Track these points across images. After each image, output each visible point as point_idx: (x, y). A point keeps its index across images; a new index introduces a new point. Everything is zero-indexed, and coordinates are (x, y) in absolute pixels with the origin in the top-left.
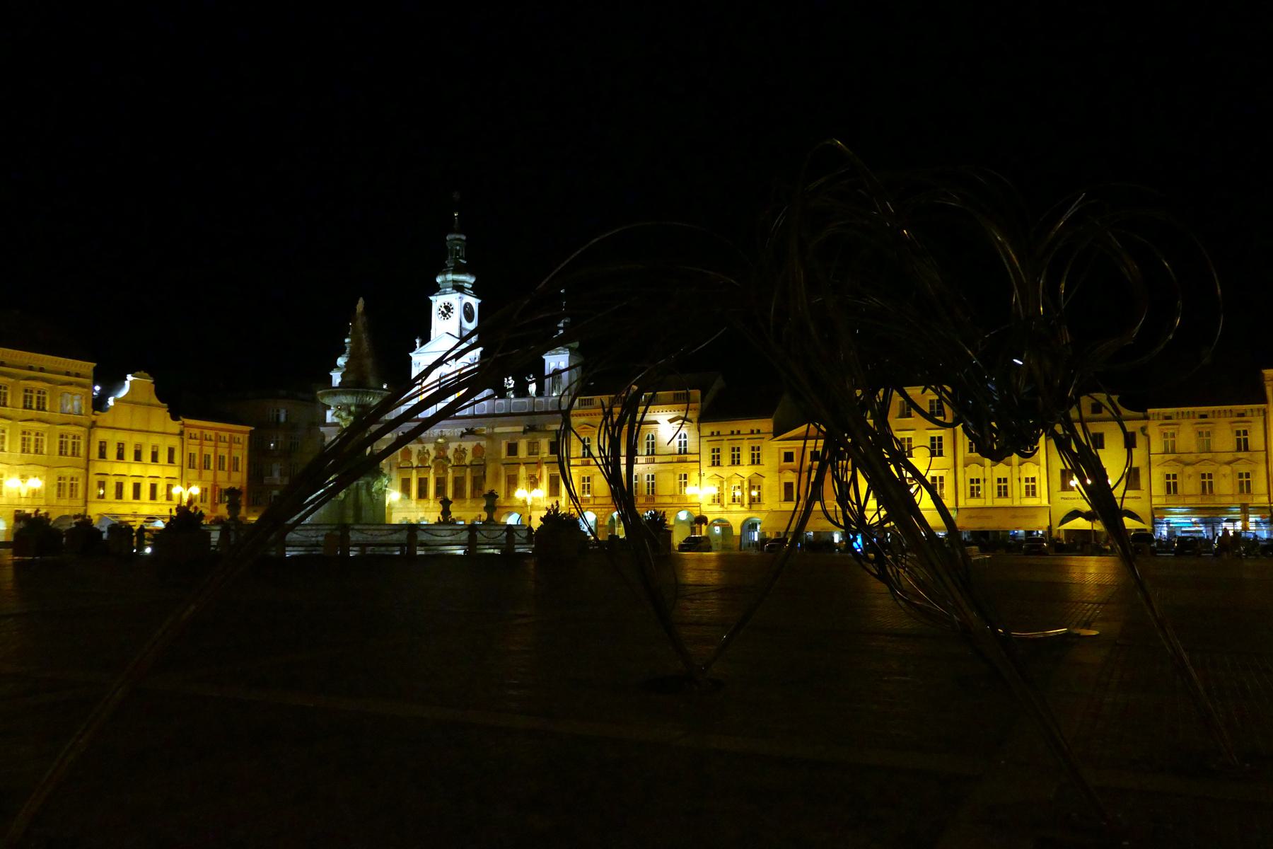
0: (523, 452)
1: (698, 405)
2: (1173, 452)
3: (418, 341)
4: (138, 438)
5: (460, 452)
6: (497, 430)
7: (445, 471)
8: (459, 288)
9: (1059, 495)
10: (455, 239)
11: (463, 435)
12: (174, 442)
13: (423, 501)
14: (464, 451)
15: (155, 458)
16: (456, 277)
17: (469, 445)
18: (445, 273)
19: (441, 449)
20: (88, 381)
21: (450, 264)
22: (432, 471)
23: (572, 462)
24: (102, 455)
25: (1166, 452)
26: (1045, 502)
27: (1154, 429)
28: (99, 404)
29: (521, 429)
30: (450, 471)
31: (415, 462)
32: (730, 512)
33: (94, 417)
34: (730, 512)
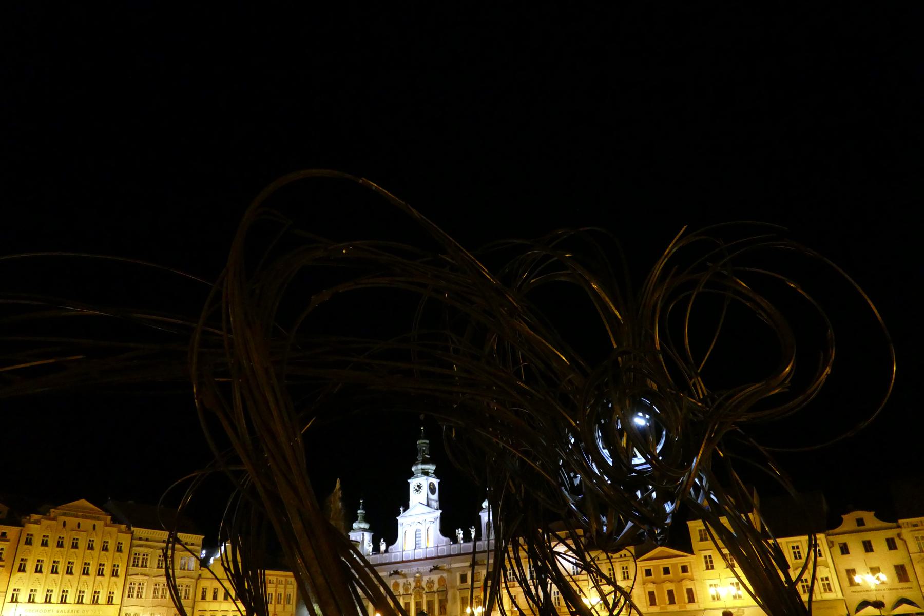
3: (402, 509)
5: (430, 583)
6: (454, 566)
7: (422, 597)
8: (426, 473)
9: (849, 590)
10: (423, 443)
14: (433, 582)
17: (435, 577)
18: (417, 464)
19: (418, 581)
20: (199, 548)
21: (420, 458)
24: (203, 598)
26: (840, 596)
29: (468, 564)
31: (402, 591)
33: (200, 572)
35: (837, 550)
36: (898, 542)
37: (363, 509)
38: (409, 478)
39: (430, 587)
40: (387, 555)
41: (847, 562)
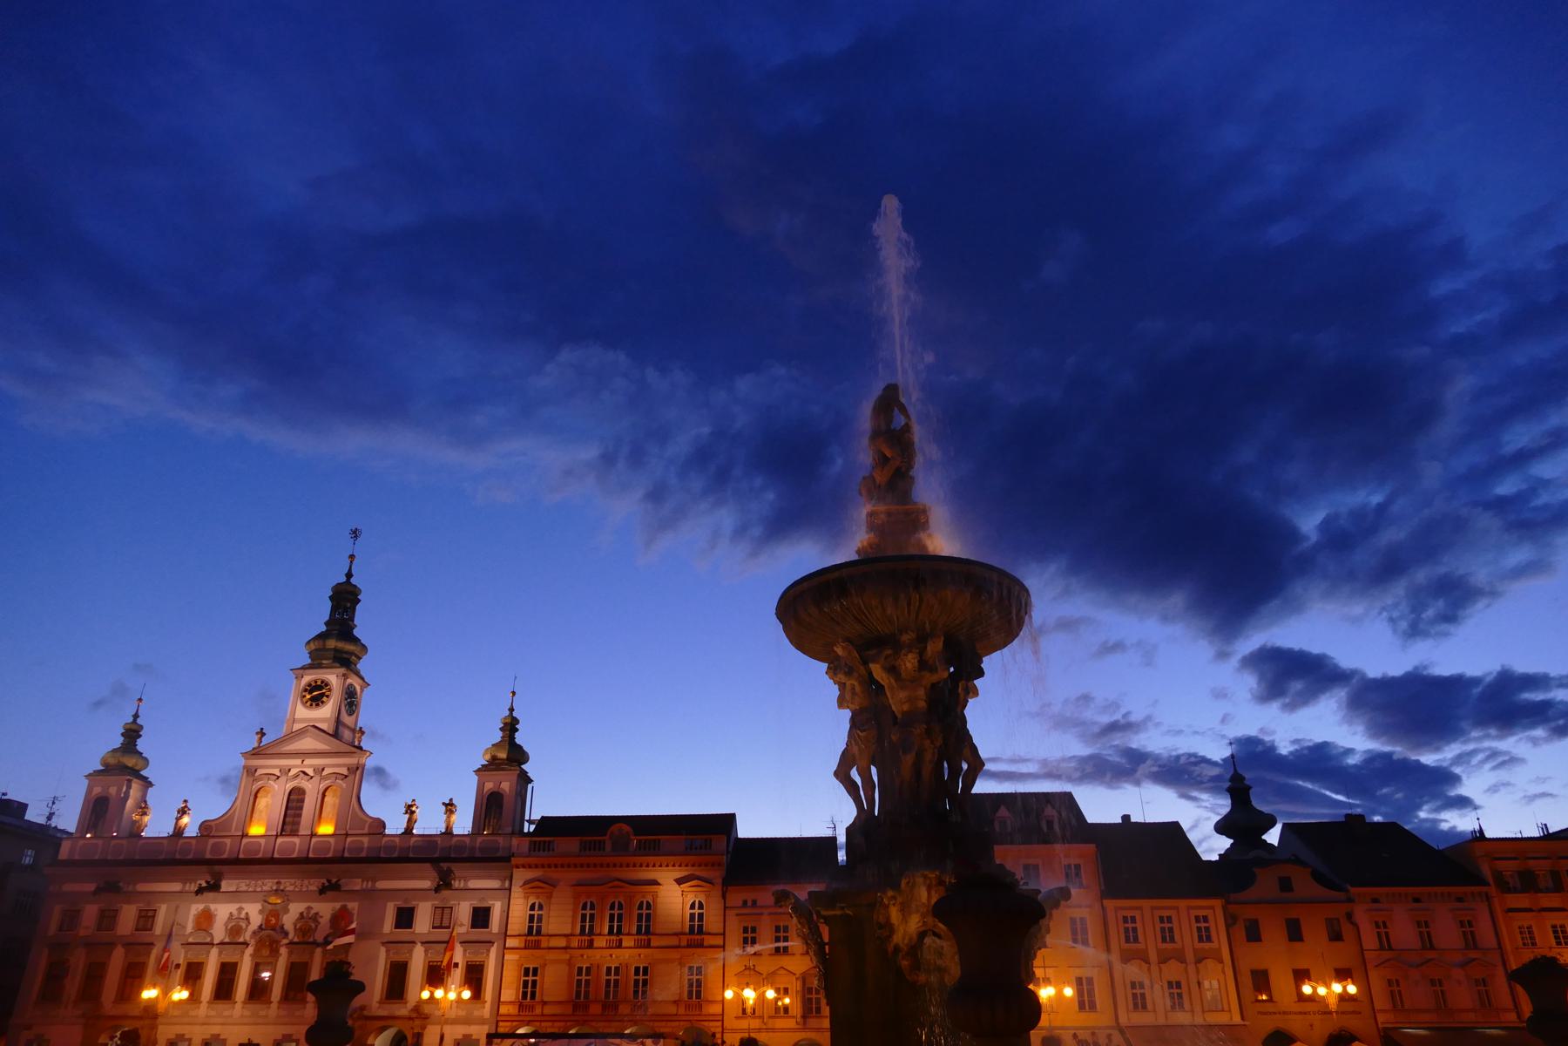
0: (423, 923)
2: (1390, 949)
5: (307, 923)
6: (381, 885)
11: (322, 891)
13: (222, 1007)
16: (340, 645)
17: (325, 909)
22: (250, 950)
23: (510, 943)
25: (1382, 948)
27: (1362, 915)
30: (283, 951)
31: (219, 933)
32: (773, 1030)
34: (773, 1030)
35: (1240, 933)
36: (1347, 930)
41: (1254, 958)
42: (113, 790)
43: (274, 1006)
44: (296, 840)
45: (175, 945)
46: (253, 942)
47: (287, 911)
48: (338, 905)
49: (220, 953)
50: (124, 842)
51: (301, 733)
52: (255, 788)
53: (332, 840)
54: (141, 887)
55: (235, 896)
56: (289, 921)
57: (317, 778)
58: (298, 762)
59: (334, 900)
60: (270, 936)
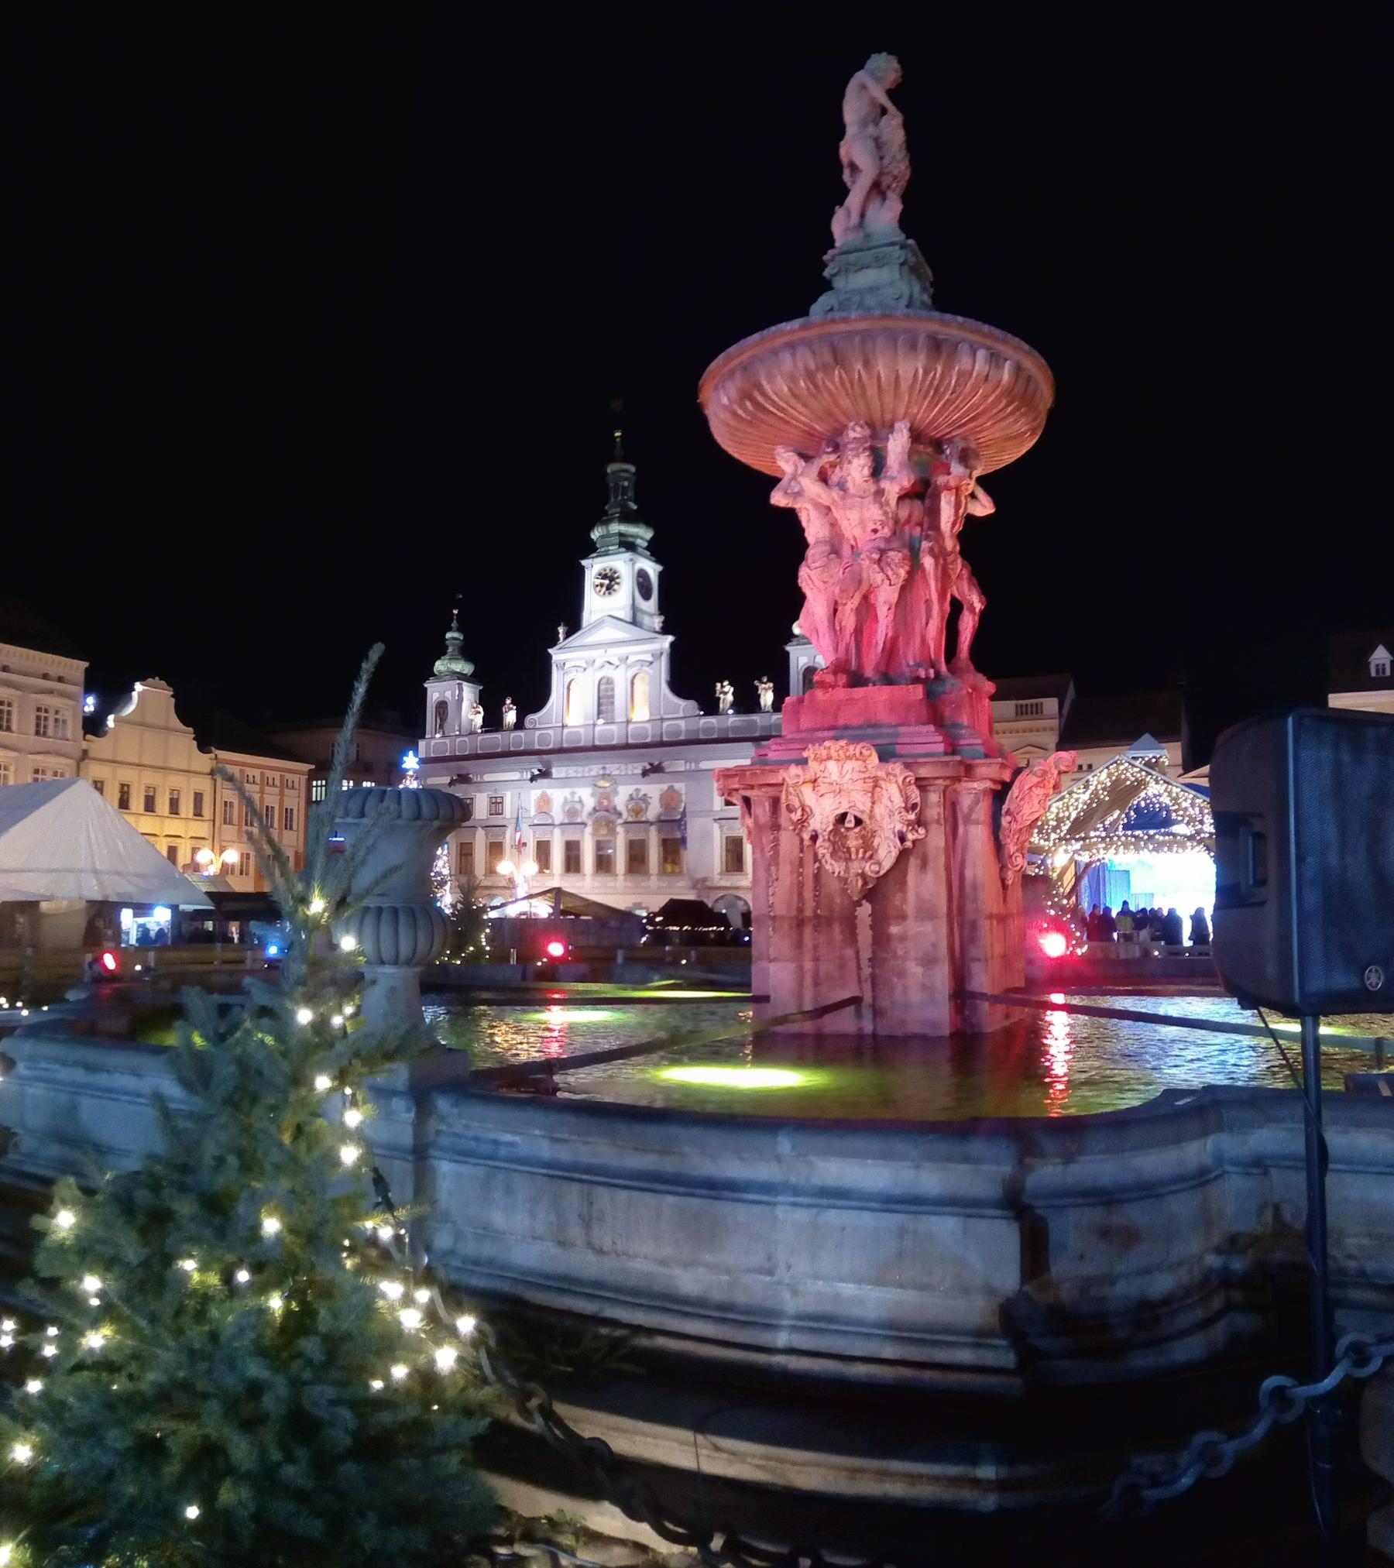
1: (1055, 723)
3: (561, 630)
4: (150, 778)
5: (639, 803)
6: (704, 765)
7: (612, 831)
11: (645, 773)
12: (204, 785)
15: (174, 807)
17: (654, 790)
21: (614, 510)
22: (589, 830)
28: (93, 725)
30: (620, 830)
31: (558, 816)
37: (459, 630)
38: (586, 557)
39: (637, 811)
40: (521, 734)
42: (448, 694)
43: (621, 878)
44: (614, 727)
45: (524, 826)
46: (590, 822)
47: (616, 793)
48: (665, 787)
49: (563, 833)
50: (466, 739)
51: (599, 623)
52: (567, 679)
53: (648, 725)
54: (487, 777)
55: (566, 781)
56: (620, 801)
57: (622, 667)
58: (601, 652)
59: (660, 782)
60: (605, 815)
